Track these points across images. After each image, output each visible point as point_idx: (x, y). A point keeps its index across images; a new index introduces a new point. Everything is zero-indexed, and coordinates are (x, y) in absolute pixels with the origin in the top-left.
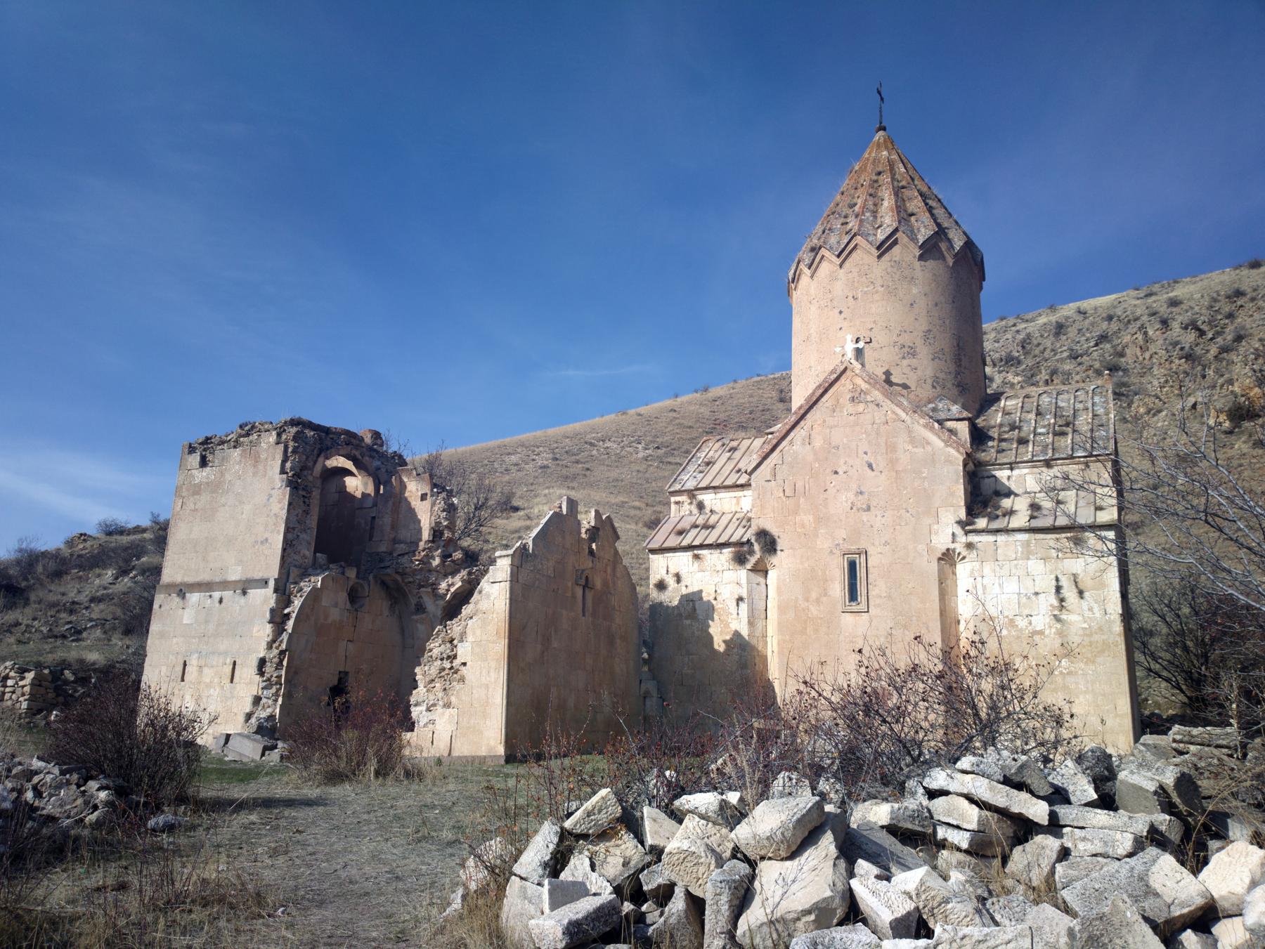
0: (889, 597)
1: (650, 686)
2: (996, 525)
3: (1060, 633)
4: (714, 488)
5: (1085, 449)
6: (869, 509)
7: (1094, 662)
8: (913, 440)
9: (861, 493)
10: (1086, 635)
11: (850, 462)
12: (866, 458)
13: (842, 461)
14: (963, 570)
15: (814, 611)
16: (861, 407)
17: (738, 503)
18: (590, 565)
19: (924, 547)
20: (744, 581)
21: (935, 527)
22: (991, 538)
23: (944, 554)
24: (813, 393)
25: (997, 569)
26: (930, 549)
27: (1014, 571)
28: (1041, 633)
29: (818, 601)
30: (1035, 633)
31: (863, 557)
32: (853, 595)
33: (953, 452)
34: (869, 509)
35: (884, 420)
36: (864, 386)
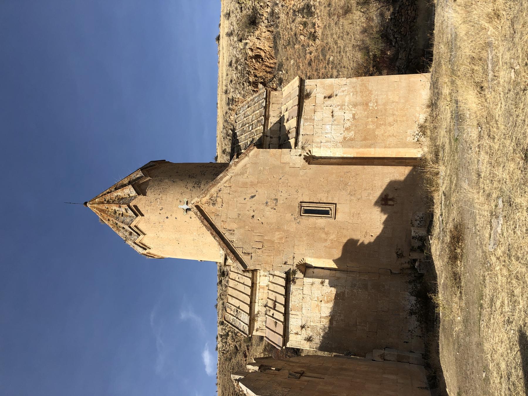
0: (328, 192)
1: (377, 353)
2: (294, 134)
3: (355, 105)
4: (251, 302)
5: (263, 102)
6: (276, 200)
7: (371, 91)
8: (242, 174)
9: (267, 203)
10: (357, 94)
11: (248, 208)
12: (248, 199)
13: (247, 213)
14: (317, 152)
15: (332, 237)
16: (219, 200)
17: (263, 288)
18: (287, 371)
19: (301, 171)
20: (310, 280)
21: (291, 164)
22: (301, 138)
23: (306, 161)
24: (205, 226)
25: (317, 135)
26: (303, 168)
27: (319, 127)
28: (354, 115)
29: (327, 234)
30: (354, 118)
31: (304, 204)
32: (326, 213)
33: (251, 153)
34: (276, 200)
35: (228, 188)
36: (208, 197)
